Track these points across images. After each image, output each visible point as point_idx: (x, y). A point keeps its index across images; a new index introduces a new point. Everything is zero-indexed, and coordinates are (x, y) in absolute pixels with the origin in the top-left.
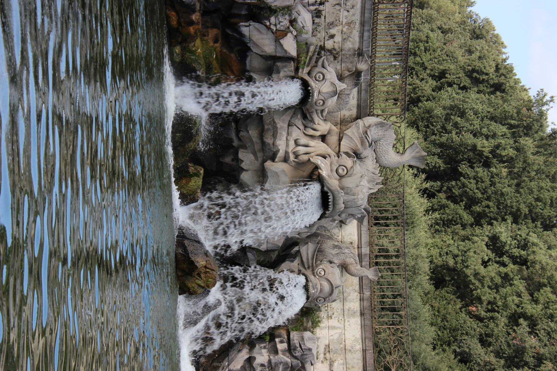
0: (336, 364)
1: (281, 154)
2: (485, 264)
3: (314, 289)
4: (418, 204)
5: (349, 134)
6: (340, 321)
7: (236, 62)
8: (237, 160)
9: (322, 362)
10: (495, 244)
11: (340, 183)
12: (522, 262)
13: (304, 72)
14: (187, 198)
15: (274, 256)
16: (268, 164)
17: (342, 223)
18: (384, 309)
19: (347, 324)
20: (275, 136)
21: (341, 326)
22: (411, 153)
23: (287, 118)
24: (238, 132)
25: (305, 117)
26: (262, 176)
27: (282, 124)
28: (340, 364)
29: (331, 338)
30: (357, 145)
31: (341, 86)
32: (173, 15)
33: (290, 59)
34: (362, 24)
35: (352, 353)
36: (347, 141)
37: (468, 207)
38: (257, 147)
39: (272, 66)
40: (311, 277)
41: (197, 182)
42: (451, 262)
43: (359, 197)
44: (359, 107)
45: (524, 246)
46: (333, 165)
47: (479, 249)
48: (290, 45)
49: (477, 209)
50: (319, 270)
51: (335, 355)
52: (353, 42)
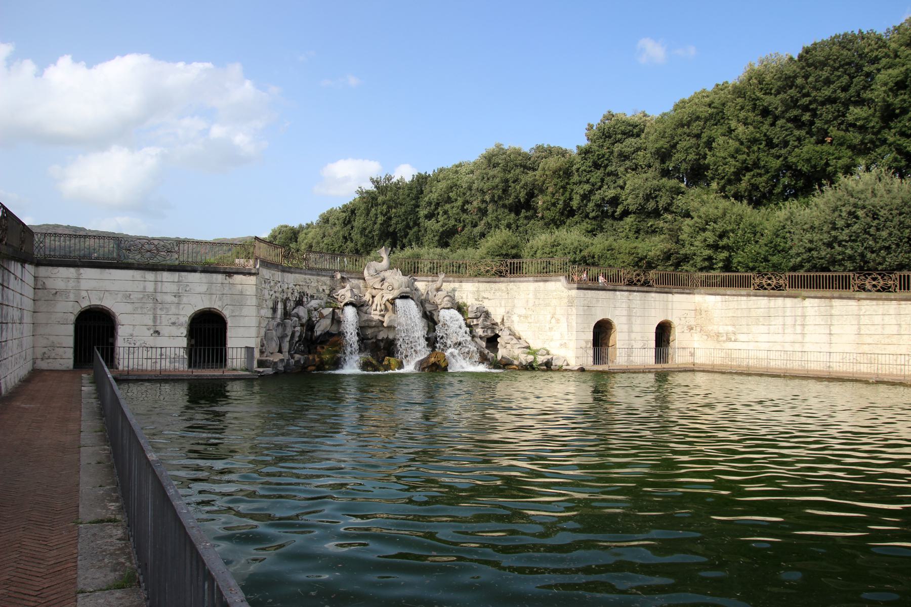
1: (380, 318)
2: (438, 222)
4: (408, 252)
7: (334, 338)
8: (382, 340)
10: (429, 217)
12: (438, 205)
14: (401, 365)
15: (431, 324)
16: (385, 324)
17: (416, 289)
18: (458, 271)
20: (371, 321)
23: (362, 314)
24: (368, 339)
25: (362, 306)
26: (391, 328)
27: (365, 317)
31: (348, 286)
32: (310, 368)
33: (333, 311)
34: (318, 275)
37: (410, 229)
38: (376, 330)
39: (336, 320)
40: (442, 306)
41: (393, 361)
42: (437, 238)
44: (359, 278)
45: (429, 203)
47: (431, 224)
48: (327, 311)
49: (411, 224)
50: (439, 302)
52: (327, 280)
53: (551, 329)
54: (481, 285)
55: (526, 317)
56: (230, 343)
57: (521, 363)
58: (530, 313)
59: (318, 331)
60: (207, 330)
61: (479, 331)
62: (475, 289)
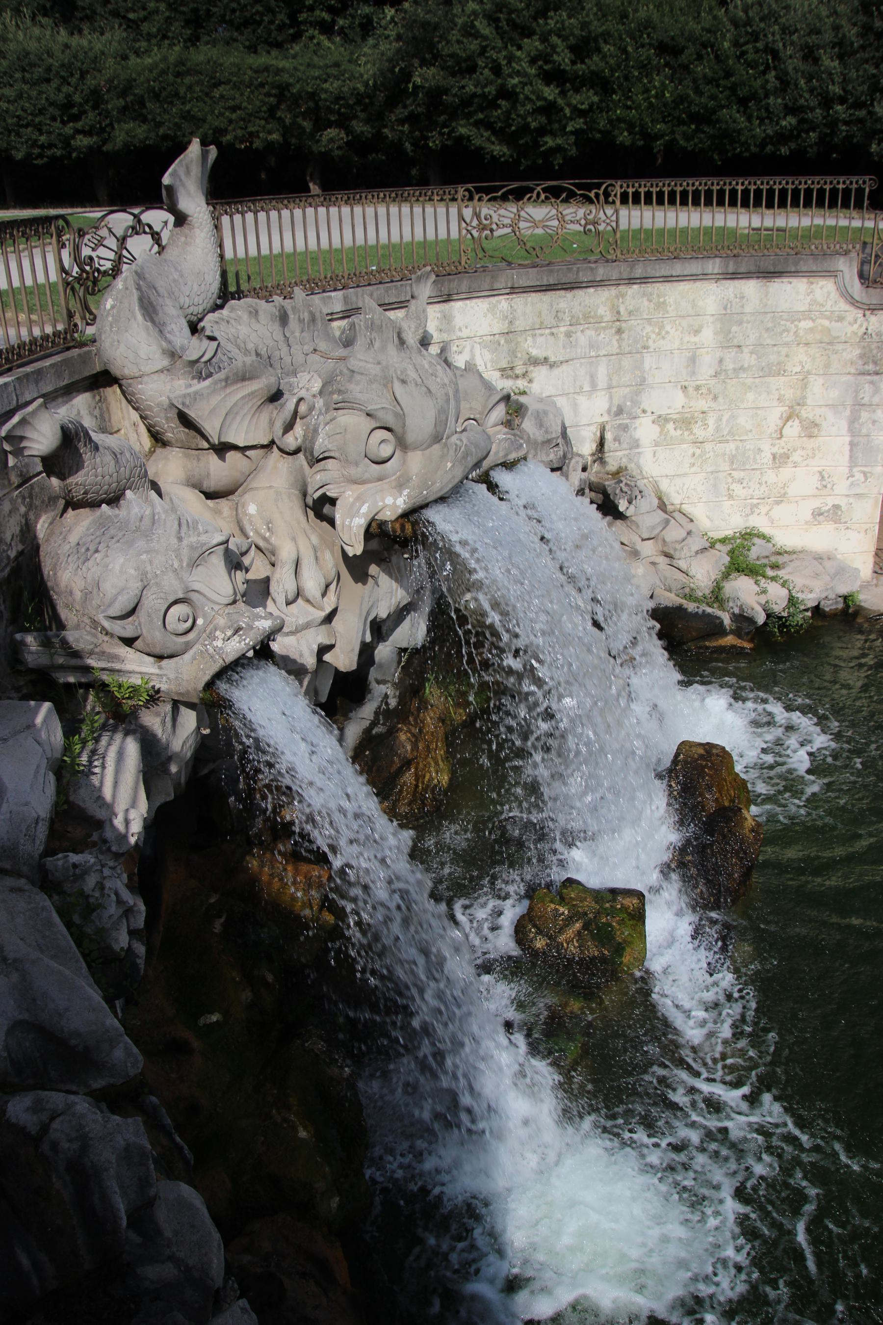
0: (535, 352)
3: (521, 445)
5: (217, 424)
6: (460, 349)
9: (530, 381)
11: (415, 448)
13: (156, 671)
19: (465, 333)
21: (468, 344)
22: (188, 193)
28: (534, 342)
29: (489, 365)
30: (252, 393)
35: (514, 318)
36: (235, 426)
43: (446, 381)
46: (367, 476)
51: (519, 355)
53: (780, 460)
54: (519, 301)
55: (685, 422)
57: (742, 619)
58: (702, 404)
62: (499, 327)
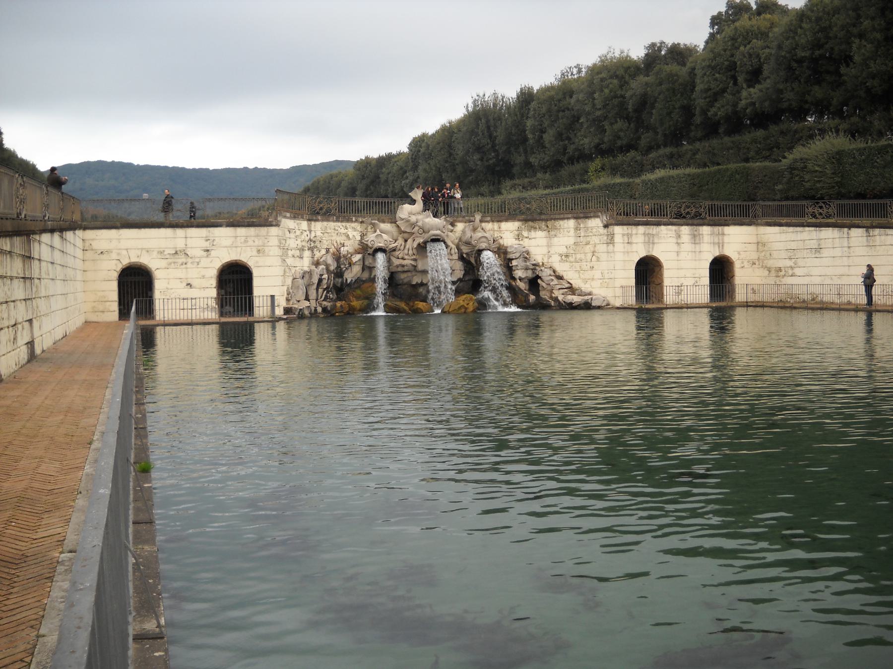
1: (413, 263)
25: (394, 250)
26: (425, 272)
27: (396, 262)
38: (409, 274)
56: (256, 292)
59: (350, 276)
60: (235, 281)
61: (519, 273)
